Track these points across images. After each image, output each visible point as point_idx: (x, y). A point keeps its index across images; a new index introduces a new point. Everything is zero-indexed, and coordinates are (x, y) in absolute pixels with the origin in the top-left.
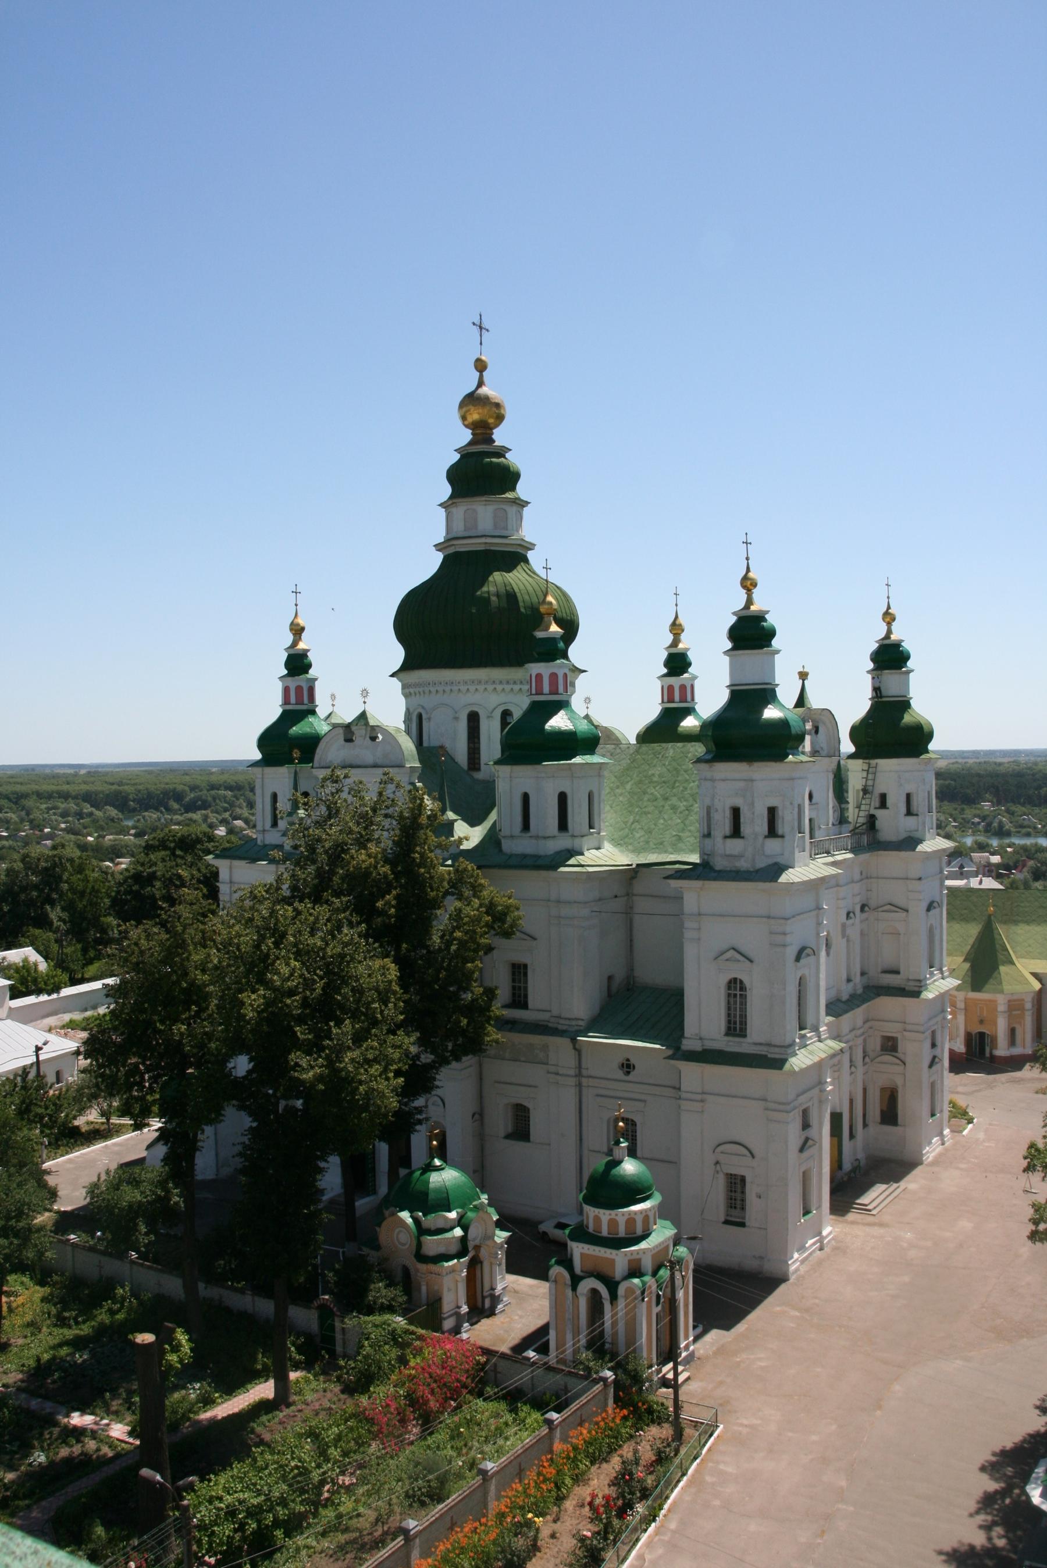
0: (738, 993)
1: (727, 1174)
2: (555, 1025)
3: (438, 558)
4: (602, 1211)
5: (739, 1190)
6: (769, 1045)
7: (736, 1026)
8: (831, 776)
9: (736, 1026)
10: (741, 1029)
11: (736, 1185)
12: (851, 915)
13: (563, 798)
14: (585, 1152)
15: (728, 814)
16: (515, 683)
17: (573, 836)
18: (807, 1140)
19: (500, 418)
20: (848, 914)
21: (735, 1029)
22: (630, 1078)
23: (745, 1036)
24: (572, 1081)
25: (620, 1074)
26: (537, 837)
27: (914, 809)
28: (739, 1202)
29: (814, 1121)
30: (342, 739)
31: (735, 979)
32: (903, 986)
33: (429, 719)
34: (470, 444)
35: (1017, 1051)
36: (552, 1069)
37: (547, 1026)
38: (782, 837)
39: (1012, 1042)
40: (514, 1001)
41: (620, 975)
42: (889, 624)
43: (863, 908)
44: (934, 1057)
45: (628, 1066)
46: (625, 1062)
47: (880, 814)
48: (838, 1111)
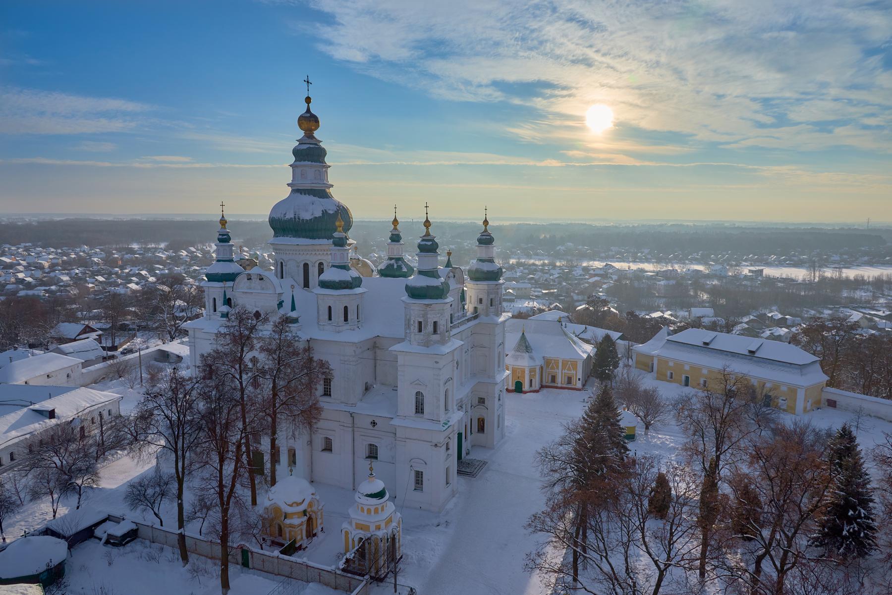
3: (290, 189)
5: (420, 477)
11: (419, 476)
15: (417, 325)
16: (324, 251)
19: (317, 127)
24: (350, 429)
25: (371, 427)
29: (451, 446)
33: (286, 266)
35: (533, 388)
36: (341, 424)
39: (531, 385)
42: (486, 226)
45: (374, 423)
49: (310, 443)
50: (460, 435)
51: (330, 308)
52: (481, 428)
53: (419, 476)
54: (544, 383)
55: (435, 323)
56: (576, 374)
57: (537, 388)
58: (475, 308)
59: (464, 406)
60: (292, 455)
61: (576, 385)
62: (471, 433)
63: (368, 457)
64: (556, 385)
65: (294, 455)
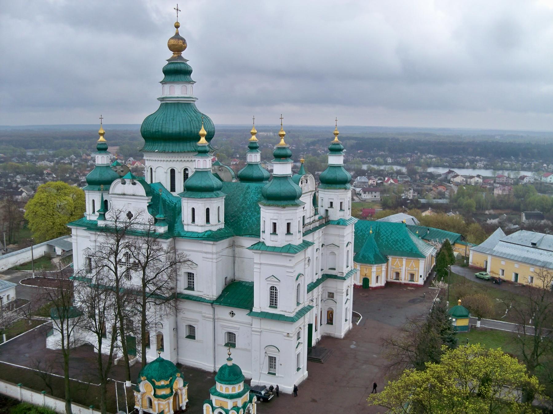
0: (274, 291)
1: (269, 356)
2: (205, 298)
3: (159, 103)
4: (223, 385)
5: (274, 362)
6: (286, 311)
7: (273, 303)
8: (312, 198)
9: (273, 303)
10: (275, 305)
11: (272, 360)
12: (318, 250)
13: (208, 210)
14: (216, 345)
17: (212, 225)
18: (299, 343)
20: (317, 250)
21: (273, 304)
22: (234, 318)
23: (276, 308)
25: (229, 317)
26: (197, 225)
27: (343, 208)
28: (273, 366)
29: (302, 335)
30: (121, 183)
31: (273, 287)
32: (336, 275)
33: (155, 172)
34: (172, 59)
36: (203, 314)
37: (202, 297)
38: (292, 234)
39: (377, 281)
40: (189, 286)
41: (230, 277)
43: (322, 246)
44: (347, 299)
45: (233, 314)
46: (232, 312)
47: (330, 210)
48: (311, 323)
49: (176, 329)
50: (310, 326)
51: (193, 210)
52: (330, 321)
53: (272, 360)
54: (389, 280)
55: (288, 225)
56: (418, 271)
57: (383, 284)
58: (327, 211)
59: (315, 301)
60: (160, 339)
61: (417, 281)
62: (321, 325)
63: (226, 345)
64: (400, 281)
65: (162, 339)
